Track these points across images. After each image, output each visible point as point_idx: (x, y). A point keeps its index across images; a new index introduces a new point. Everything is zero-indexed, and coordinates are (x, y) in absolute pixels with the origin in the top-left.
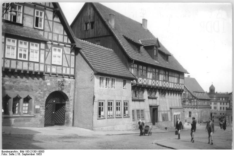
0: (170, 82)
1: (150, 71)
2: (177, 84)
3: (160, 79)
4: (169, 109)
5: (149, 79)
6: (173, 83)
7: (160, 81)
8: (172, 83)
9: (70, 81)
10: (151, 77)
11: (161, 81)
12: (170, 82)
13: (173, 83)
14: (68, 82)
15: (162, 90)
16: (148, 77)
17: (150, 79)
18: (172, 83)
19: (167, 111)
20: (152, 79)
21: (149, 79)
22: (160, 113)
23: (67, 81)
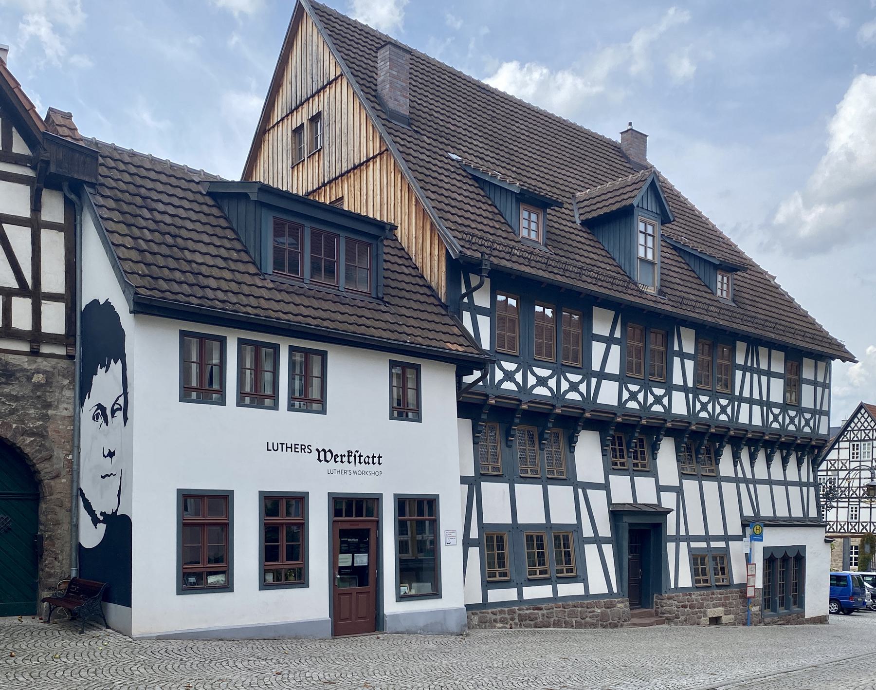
0: (741, 399)
1: (606, 333)
2: (785, 407)
3: (677, 379)
4: (735, 528)
5: (602, 375)
6: (760, 403)
7: (678, 388)
8: (751, 401)
9: (45, 372)
10: (613, 366)
11: (684, 389)
12: (741, 399)
13: (760, 403)
14: (29, 379)
15: (697, 435)
16: (596, 366)
17: (611, 377)
18: (751, 401)
19: (727, 538)
20: (622, 379)
21: (602, 375)
22: (683, 546)
23: (27, 371)
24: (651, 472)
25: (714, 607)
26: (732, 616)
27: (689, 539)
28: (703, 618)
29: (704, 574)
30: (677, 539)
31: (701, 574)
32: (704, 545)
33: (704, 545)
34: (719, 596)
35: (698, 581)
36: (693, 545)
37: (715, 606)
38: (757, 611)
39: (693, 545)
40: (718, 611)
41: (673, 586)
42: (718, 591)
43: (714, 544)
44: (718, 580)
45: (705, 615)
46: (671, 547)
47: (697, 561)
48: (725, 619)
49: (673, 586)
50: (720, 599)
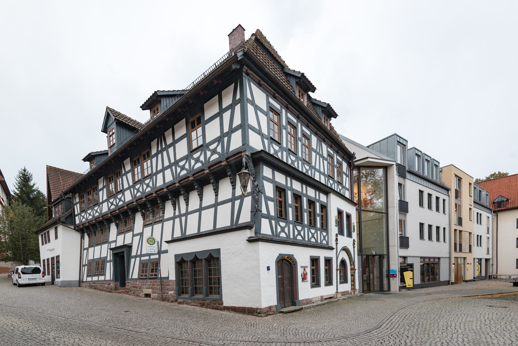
22: (138, 259)
24: (132, 229)
25: (147, 289)
26: (156, 294)
27: (141, 256)
28: (141, 293)
29: (146, 272)
30: (136, 257)
31: (144, 272)
32: (147, 258)
33: (147, 258)
34: (149, 283)
35: (142, 276)
36: (143, 258)
37: (147, 288)
38: (172, 294)
39: (143, 258)
40: (149, 291)
41: (130, 278)
42: (149, 281)
43: (152, 257)
44: (152, 275)
45: (142, 291)
46: (133, 260)
47: (143, 265)
48: (153, 295)
49: (130, 278)
50: (150, 285)
